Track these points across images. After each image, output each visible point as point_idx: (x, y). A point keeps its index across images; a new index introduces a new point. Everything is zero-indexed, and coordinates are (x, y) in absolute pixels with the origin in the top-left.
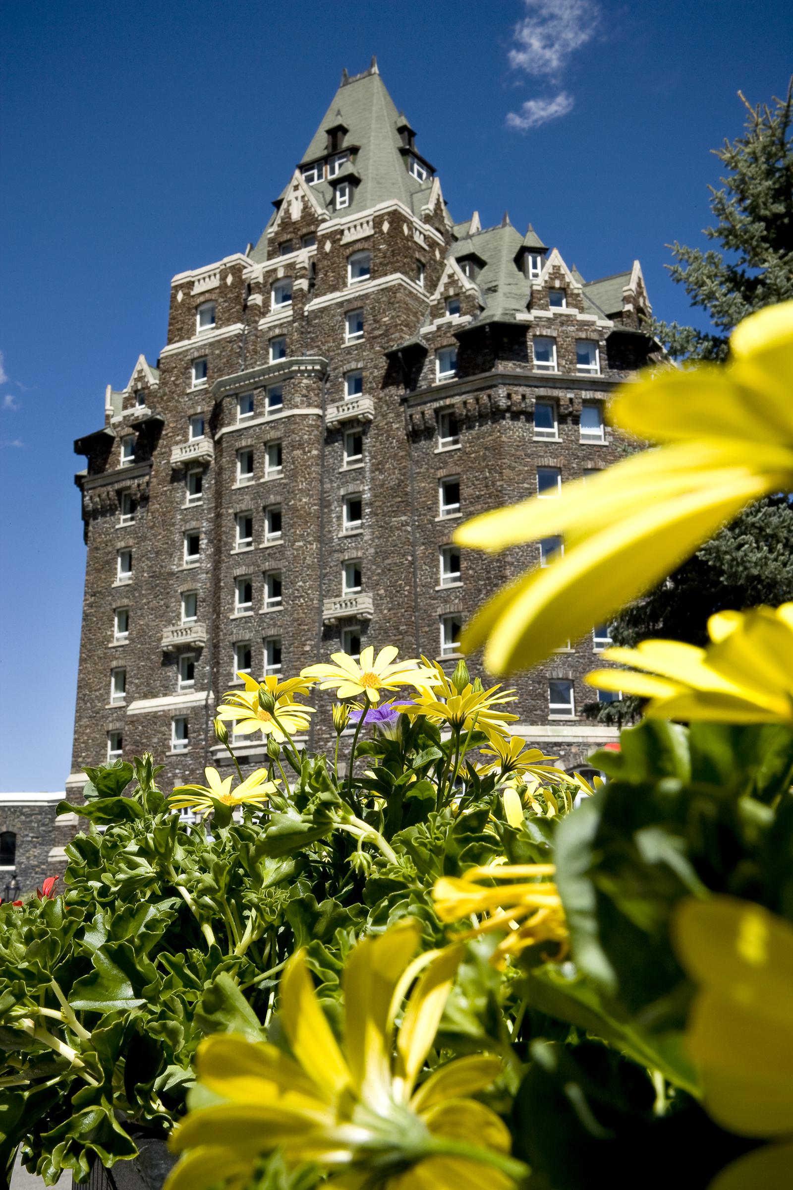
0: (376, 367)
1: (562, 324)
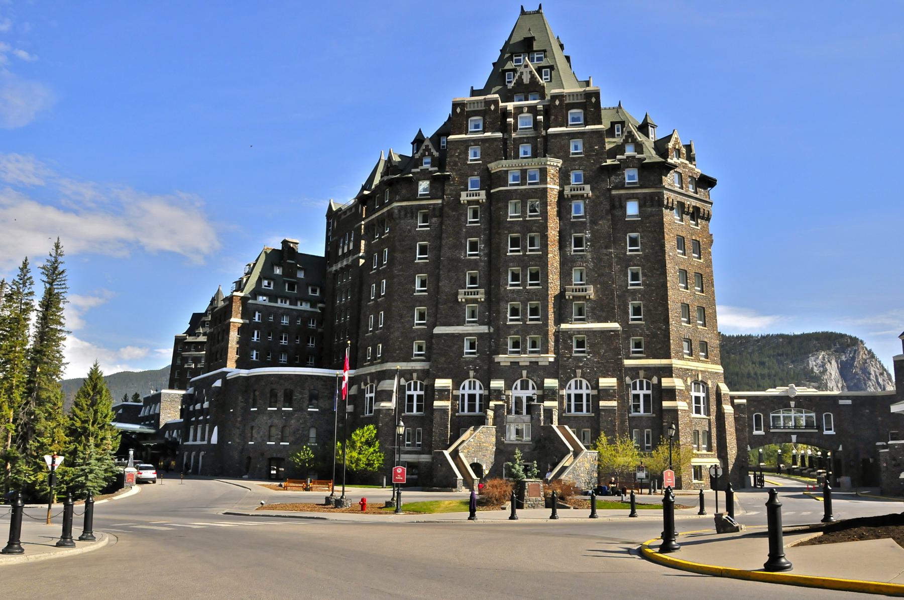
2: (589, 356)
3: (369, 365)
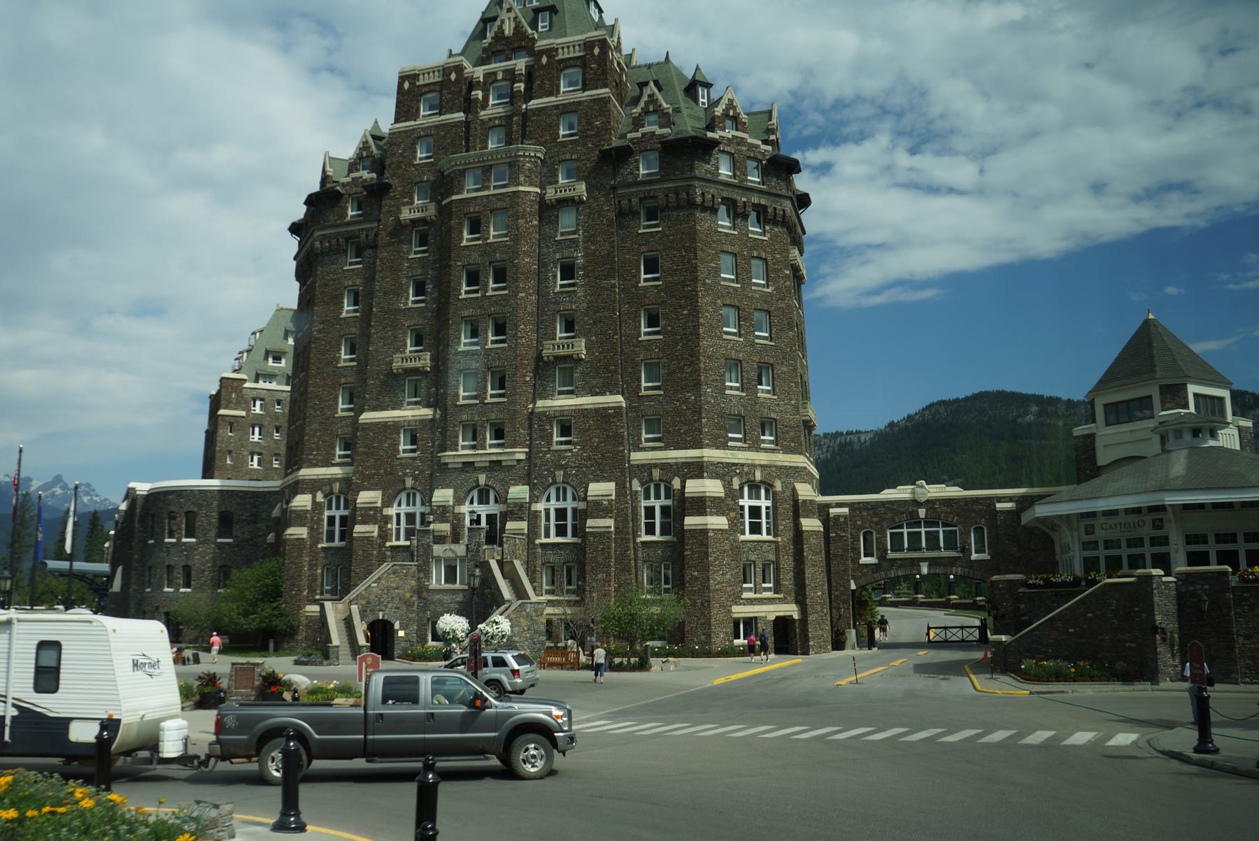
0: (588, 160)
1: (738, 144)
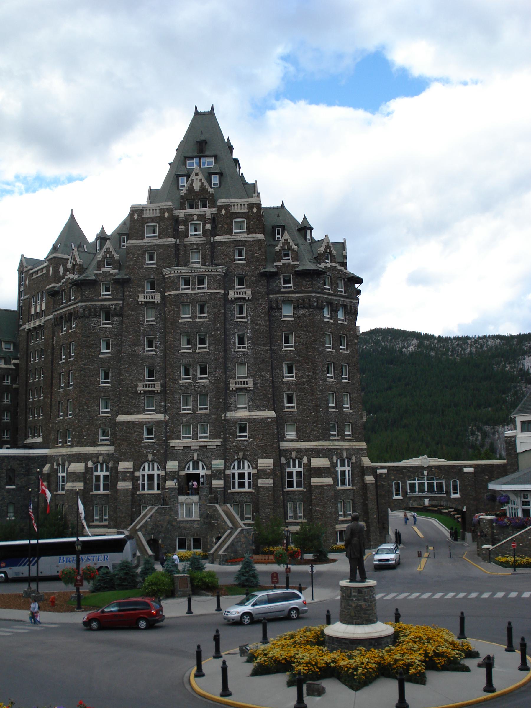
0: (252, 276)
2: (249, 440)
3: (60, 447)
